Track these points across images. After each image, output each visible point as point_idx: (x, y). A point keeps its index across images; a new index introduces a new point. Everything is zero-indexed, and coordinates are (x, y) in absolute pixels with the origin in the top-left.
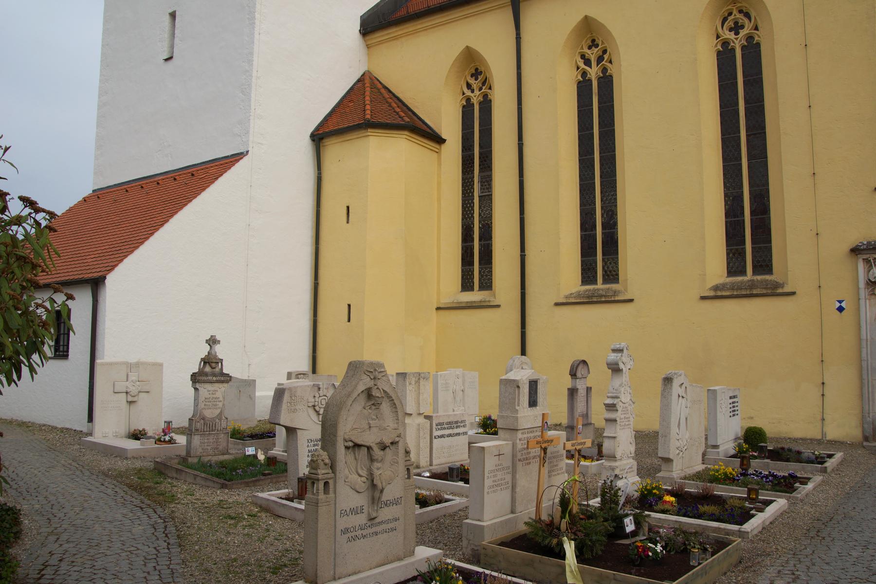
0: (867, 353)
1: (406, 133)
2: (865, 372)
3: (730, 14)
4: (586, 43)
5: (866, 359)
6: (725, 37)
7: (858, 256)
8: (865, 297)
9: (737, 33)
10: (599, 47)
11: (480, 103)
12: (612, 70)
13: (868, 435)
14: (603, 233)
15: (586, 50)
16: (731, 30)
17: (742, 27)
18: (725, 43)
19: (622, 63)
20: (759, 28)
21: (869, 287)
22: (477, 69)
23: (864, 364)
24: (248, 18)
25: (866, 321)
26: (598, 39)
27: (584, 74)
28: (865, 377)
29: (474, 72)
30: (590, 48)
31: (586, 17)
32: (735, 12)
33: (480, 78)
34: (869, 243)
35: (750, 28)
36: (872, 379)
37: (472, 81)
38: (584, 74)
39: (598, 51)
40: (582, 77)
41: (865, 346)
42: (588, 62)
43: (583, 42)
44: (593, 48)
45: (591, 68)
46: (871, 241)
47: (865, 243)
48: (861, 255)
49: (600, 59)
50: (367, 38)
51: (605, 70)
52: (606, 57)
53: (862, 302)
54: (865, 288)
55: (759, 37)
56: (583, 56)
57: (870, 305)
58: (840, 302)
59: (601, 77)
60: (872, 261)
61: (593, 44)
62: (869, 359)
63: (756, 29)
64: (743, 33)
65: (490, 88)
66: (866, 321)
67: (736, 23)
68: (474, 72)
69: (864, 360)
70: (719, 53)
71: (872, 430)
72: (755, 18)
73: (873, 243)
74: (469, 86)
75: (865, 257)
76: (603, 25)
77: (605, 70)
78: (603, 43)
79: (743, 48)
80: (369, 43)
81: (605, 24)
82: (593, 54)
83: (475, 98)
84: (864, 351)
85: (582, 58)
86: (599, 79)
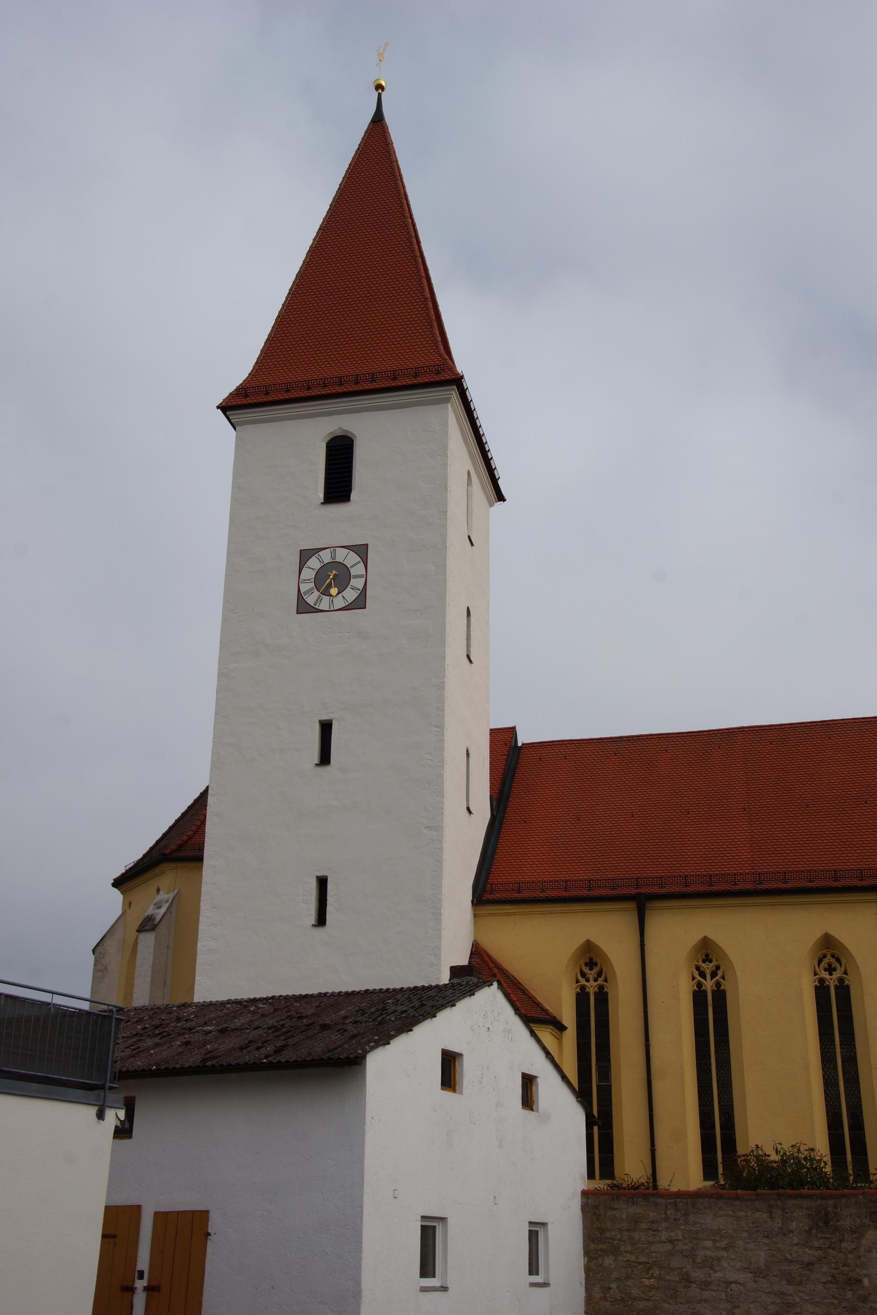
1: (551, 1027)
3: (825, 956)
4: (701, 957)
6: (822, 976)
9: (831, 974)
10: (714, 963)
11: (596, 994)
12: (726, 986)
14: (721, 1133)
15: (701, 964)
16: (825, 970)
17: (835, 970)
18: (822, 981)
19: (739, 986)
20: (849, 972)
22: (591, 959)
24: (432, 913)
26: (712, 955)
27: (699, 985)
29: (588, 961)
30: (704, 961)
31: (705, 937)
32: (829, 956)
33: (596, 970)
35: (842, 972)
37: (586, 970)
38: (699, 985)
39: (712, 967)
40: (697, 987)
42: (703, 975)
43: (699, 956)
44: (707, 963)
45: (706, 980)
49: (714, 974)
50: (477, 908)
51: (718, 984)
52: (720, 973)
55: (849, 981)
56: (698, 968)
59: (715, 991)
61: (707, 959)
63: (846, 973)
64: (836, 975)
65: (606, 981)
67: (830, 965)
68: (588, 961)
70: (816, 988)
72: (845, 966)
74: (583, 975)
76: (720, 948)
77: (718, 984)
78: (717, 960)
79: (836, 987)
80: (477, 912)
81: (724, 948)
82: (708, 968)
83: (591, 989)
85: (697, 970)
86: (713, 992)
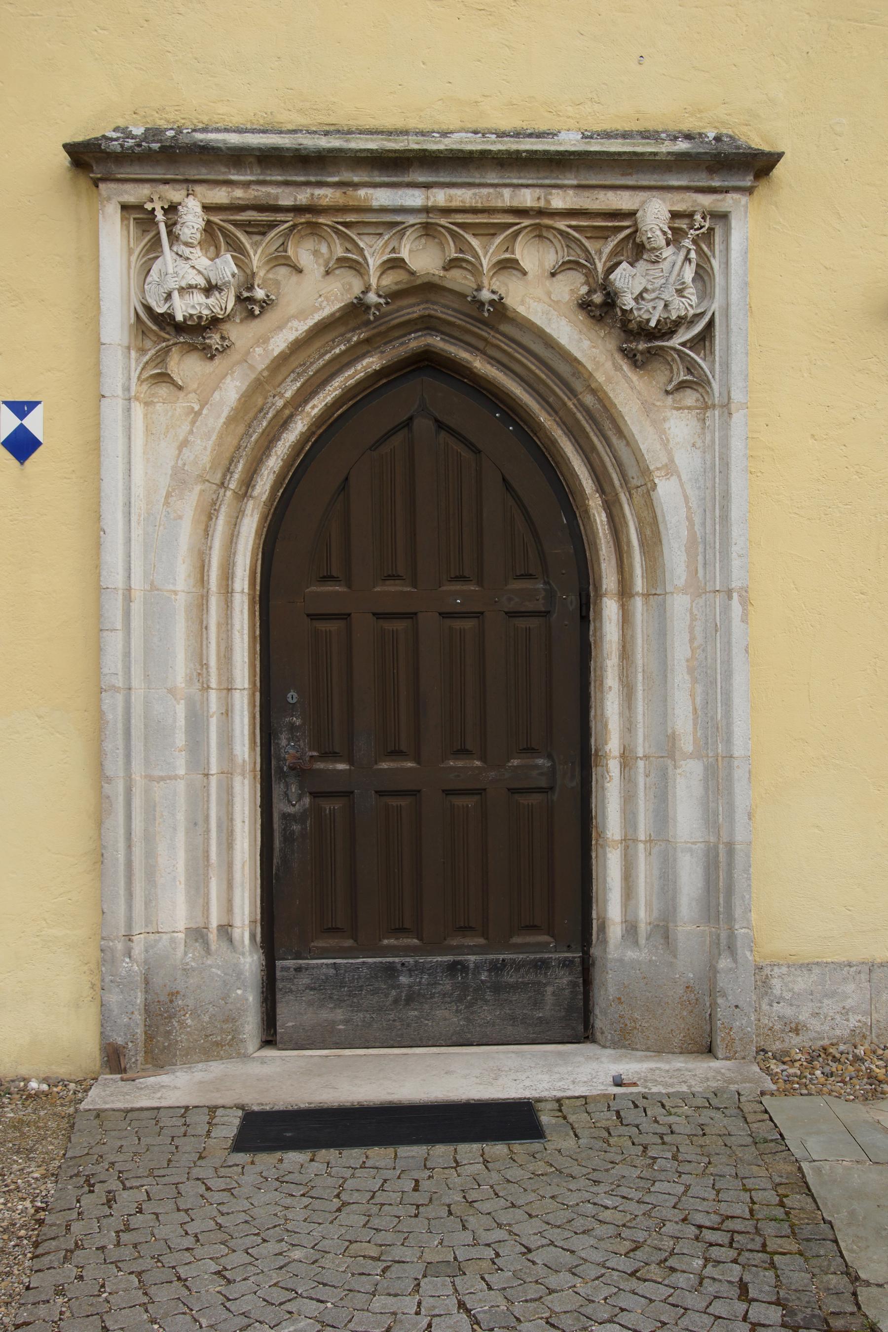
0: (127, 654)
2: (114, 744)
5: (119, 682)
7: (102, 186)
8: (127, 389)
13: (120, 1041)
21: (148, 344)
23: (114, 705)
25: (128, 504)
28: (115, 767)
34: (153, 133)
36: (150, 778)
41: (119, 625)
46: (163, 124)
47: (138, 131)
48: (112, 186)
53: (113, 410)
54: (129, 348)
57: (147, 429)
58: (21, 409)
60: (160, 216)
62: (137, 682)
66: (128, 504)
69: (114, 689)
71: (138, 1017)
73: (170, 133)
75: (133, 194)
84: (114, 642)
